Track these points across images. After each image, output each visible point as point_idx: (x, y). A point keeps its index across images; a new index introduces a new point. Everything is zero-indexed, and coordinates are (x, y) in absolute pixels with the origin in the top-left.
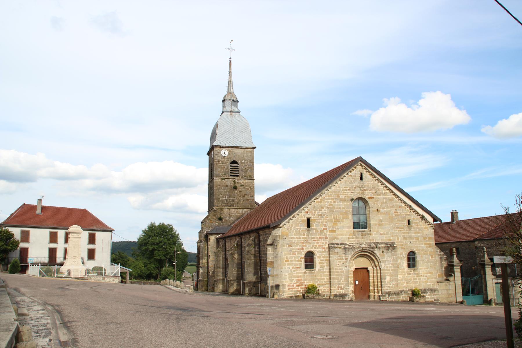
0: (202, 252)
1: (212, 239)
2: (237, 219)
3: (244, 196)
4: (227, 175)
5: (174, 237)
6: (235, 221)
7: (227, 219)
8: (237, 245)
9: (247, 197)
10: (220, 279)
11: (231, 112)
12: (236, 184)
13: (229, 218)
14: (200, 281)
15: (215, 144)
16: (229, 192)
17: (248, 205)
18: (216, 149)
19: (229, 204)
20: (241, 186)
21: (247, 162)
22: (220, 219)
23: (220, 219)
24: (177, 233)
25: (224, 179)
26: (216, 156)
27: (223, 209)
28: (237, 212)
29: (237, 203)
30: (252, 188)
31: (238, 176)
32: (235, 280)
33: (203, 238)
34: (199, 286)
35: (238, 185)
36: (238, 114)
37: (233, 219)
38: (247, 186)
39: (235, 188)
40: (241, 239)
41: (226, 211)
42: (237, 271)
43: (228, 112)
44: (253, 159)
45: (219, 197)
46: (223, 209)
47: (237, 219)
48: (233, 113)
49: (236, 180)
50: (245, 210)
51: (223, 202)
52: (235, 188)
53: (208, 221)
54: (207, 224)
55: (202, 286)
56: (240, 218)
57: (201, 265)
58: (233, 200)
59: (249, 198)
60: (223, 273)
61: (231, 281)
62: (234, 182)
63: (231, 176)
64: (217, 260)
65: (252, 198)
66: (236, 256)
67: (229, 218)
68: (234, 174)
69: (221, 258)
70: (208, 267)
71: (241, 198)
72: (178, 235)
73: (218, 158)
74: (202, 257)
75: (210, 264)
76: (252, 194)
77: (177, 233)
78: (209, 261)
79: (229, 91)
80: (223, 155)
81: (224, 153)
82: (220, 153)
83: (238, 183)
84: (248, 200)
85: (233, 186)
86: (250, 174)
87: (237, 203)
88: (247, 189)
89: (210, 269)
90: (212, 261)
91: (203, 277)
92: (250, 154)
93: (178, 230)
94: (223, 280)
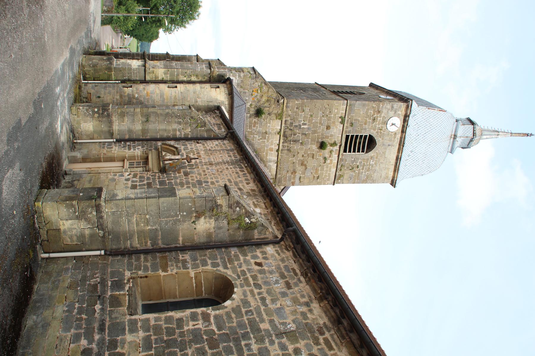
0: (182, 67)
1: (218, 95)
2: (255, 151)
3: (302, 164)
4: (350, 129)
5: (182, 22)
6: (251, 145)
7: (258, 128)
8: (251, 227)
9: (299, 169)
10: (111, 123)
11: (455, 136)
12: (329, 148)
14: (109, 60)
15: (414, 104)
16: (315, 132)
17: (284, 172)
18: (403, 105)
19: (289, 132)
20: (325, 159)
21: (368, 170)
22: (259, 113)
23: (259, 113)
24: (187, 25)
25: (342, 122)
27: (281, 119)
28: (271, 150)
29: (289, 150)
30: (317, 180)
31: (345, 151)
32: (100, 226)
33: (217, 71)
34: (96, 59)
35: (326, 152)
36: (449, 150)
37: (257, 140)
38: (322, 169)
39: (322, 146)
40: (275, 242)
41: (275, 125)
42: (141, 233)
44: (373, 182)
45: (307, 109)
46: (281, 119)
47: (255, 151)
48: (452, 139)
49: (337, 148)
50: (274, 166)
51: (293, 119)
52: (322, 146)
53: (257, 84)
54: (249, 81)
55: (94, 66)
56: (257, 155)
57: (150, 63)
58: (295, 141)
59: (297, 176)
60: (130, 131)
61: (98, 208)
62: (335, 144)
63: (347, 137)
64: (168, 112)
65: (297, 181)
66: (204, 226)
67: (259, 133)
69: (175, 126)
70: (144, 81)
71: (300, 157)
72: (185, 27)
73: (385, 111)
74: (172, 67)
75: (152, 87)
76: (306, 181)
77: (187, 25)
78: (163, 86)
79: (486, 133)
80: (390, 122)
81: (395, 123)
82: (396, 114)
83: (331, 152)
84: (294, 172)
85: (327, 141)
86: (346, 177)
87: (289, 150)
88: (317, 170)
89: (141, 86)
90: (162, 95)
91: (119, 70)
92: (383, 175)
93: (192, 26)
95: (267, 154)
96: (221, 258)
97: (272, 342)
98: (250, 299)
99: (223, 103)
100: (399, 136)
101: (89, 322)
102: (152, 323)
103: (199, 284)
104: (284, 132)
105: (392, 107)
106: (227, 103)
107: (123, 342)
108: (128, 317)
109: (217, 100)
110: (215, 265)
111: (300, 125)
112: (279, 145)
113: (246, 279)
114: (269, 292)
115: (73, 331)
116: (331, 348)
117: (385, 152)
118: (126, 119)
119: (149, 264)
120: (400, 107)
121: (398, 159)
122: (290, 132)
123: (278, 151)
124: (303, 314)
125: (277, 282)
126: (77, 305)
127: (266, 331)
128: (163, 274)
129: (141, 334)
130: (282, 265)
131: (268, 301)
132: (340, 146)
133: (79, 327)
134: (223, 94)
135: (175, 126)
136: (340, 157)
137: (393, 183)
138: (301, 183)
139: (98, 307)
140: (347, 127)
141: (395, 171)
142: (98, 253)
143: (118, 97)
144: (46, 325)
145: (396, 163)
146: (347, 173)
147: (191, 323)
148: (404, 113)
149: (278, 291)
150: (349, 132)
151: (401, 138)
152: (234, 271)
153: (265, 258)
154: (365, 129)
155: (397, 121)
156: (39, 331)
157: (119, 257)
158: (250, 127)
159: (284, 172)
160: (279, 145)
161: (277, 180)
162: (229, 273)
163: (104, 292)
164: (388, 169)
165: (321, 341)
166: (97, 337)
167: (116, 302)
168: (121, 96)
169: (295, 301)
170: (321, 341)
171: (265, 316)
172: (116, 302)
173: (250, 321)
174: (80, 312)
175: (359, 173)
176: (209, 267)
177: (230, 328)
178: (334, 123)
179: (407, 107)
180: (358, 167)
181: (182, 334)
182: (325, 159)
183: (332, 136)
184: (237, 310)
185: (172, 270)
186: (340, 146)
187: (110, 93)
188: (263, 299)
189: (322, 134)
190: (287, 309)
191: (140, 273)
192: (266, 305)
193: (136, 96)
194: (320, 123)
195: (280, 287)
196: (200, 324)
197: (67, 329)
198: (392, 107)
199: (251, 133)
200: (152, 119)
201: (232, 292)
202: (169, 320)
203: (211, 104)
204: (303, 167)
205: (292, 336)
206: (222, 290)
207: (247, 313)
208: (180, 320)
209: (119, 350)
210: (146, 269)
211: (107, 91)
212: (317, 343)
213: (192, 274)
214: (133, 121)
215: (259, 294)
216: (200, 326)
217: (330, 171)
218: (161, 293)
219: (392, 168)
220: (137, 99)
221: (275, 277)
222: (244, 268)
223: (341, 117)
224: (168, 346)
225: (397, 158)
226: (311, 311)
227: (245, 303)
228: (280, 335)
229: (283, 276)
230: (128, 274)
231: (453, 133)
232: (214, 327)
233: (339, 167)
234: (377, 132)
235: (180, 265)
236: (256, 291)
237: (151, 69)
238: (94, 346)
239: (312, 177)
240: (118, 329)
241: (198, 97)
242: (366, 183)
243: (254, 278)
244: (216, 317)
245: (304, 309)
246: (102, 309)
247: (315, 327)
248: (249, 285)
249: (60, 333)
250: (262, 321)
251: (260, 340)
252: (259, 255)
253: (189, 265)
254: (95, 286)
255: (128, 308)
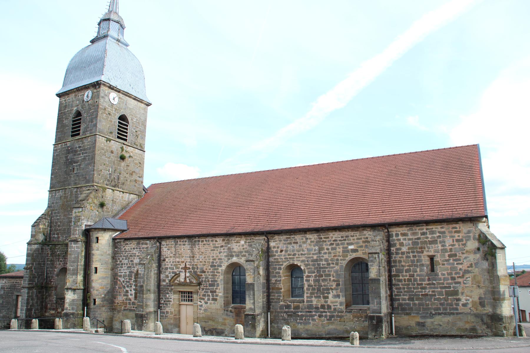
6: (119, 212)
9: (135, 177)
10: (150, 312)
13: (112, 206)
16: (114, 163)
25: (110, 140)
26: (102, 100)
27: (106, 189)
29: (123, 184)
30: (141, 164)
31: (126, 140)
35: (127, 155)
36: (125, 47)
42: (263, 298)
43: (114, 39)
44: (146, 120)
46: (106, 189)
47: (122, 209)
48: (120, 44)
50: (132, 196)
52: (122, 158)
58: (118, 179)
59: (138, 179)
62: (122, 148)
63: (118, 137)
65: (140, 179)
66: (262, 272)
67: (112, 206)
68: (122, 134)
69: (152, 274)
71: (127, 176)
73: (105, 104)
76: (141, 172)
82: (108, 95)
83: (126, 152)
84: (136, 181)
87: (123, 184)
90: (104, 278)
94: (156, 312)
95: (125, 201)
96: (276, 265)
97: (323, 256)
98: (301, 259)
99: (110, 236)
100: (121, 95)
101: (307, 316)
102: (309, 295)
103: (287, 276)
104: (113, 186)
105: (103, 97)
106: (111, 233)
107: (316, 305)
108: (305, 303)
109: (108, 240)
110: (280, 269)
111: (110, 174)
112: (120, 191)
113: (290, 258)
114: (299, 251)
115: (310, 321)
116: (328, 238)
117: (131, 108)
118: (148, 303)
119: (276, 295)
120: (103, 90)
121: (135, 99)
122: (113, 182)
123: (123, 192)
124: (311, 242)
125: (293, 247)
126: (298, 321)
127: (317, 257)
128: (283, 290)
129: (313, 299)
130: (283, 242)
131: (303, 253)
132: (124, 144)
133: (309, 319)
134: (104, 235)
135: (152, 274)
136: (129, 144)
137: (148, 105)
138: (141, 177)
139: (300, 314)
140: (112, 137)
141: (142, 102)
142: (269, 315)
143: (104, 308)
144: (307, 330)
145: (137, 100)
146: (139, 141)
147: (311, 282)
148: (107, 88)
149: (298, 248)
150: (115, 135)
151: (123, 94)
152: (285, 262)
153: (278, 247)
154: (115, 122)
155: (113, 95)
156: (309, 332)
157: (271, 306)
158: (109, 212)
159: (136, 188)
160: (120, 191)
161: (140, 194)
162: (285, 264)
163: (292, 312)
164: (140, 107)
165: (325, 240)
166: (314, 313)
167: (297, 307)
168: (103, 306)
169: (304, 243)
170: (325, 240)
171: (311, 256)
172: (297, 307)
173: (312, 261)
174: (302, 320)
175: (140, 131)
176: (281, 271)
177: (314, 269)
178: (110, 147)
179: (104, 85)
180: (136, 131)
181: (315, 286)
182: (130, 157)
183: (117, 150)
184: (306, 265)
185: (281, 285)
186: (124, 144)
187: (100, 314)
188: (302, 254)
189: (116, 157)
190: (308, 247)
191: (281, 298)
192: (305, 254)
193: (103, 296)
194: (109, 158)
195: (296, 247)
196: (312, 279)
197: (310, 323)
198: (103, 97)
199: (112, 212)
200: (148, 288)
201: (297, 265)
202: (308, 289)
203: (111, 244)
204: (134, 174)
205: (321, 249)
206: (293, 269)
207: (307, 262)
208: (309, 286)
209: (319, 306)
210: (280, 296)
211: (99, 316)
212: (326, 241)
213: (284, 278)
214: (149, 299)
215: (299, 255)
216: (312, 279)
217: (137, 154)
218: (288, 291)
219: (139, 103)
220: (105, 295)
221: (290, 247)
222: (283, 257)
223: (107, 141)
224: (320, 290)
225: (134, 99)
226: (310, 239)
227: (303, 261)
228: (320, 253)
229: (290, 243)
230: (281, 303)
231: (115, 41)
232: (314, 275)
233: (135, 147)
234: (118, 112)
235: (278, 282)
236: (297, 256)
237: (78, 285)
238: (317, 314)
239: (139, 168)
240: (310, 307)
241: (106, 253)
242: (146, 126)
243: (289, 255)
244: (309, 273)
245: (309, 241)
246: (301, 312)
247: (318, 240)
248: (294, 258)
249: (311, 325)
250: (313, 257)
251: (321, 260)
252: (275, 250)
253: (279, 279)
254: (288, 315)
255: (300, 303)
